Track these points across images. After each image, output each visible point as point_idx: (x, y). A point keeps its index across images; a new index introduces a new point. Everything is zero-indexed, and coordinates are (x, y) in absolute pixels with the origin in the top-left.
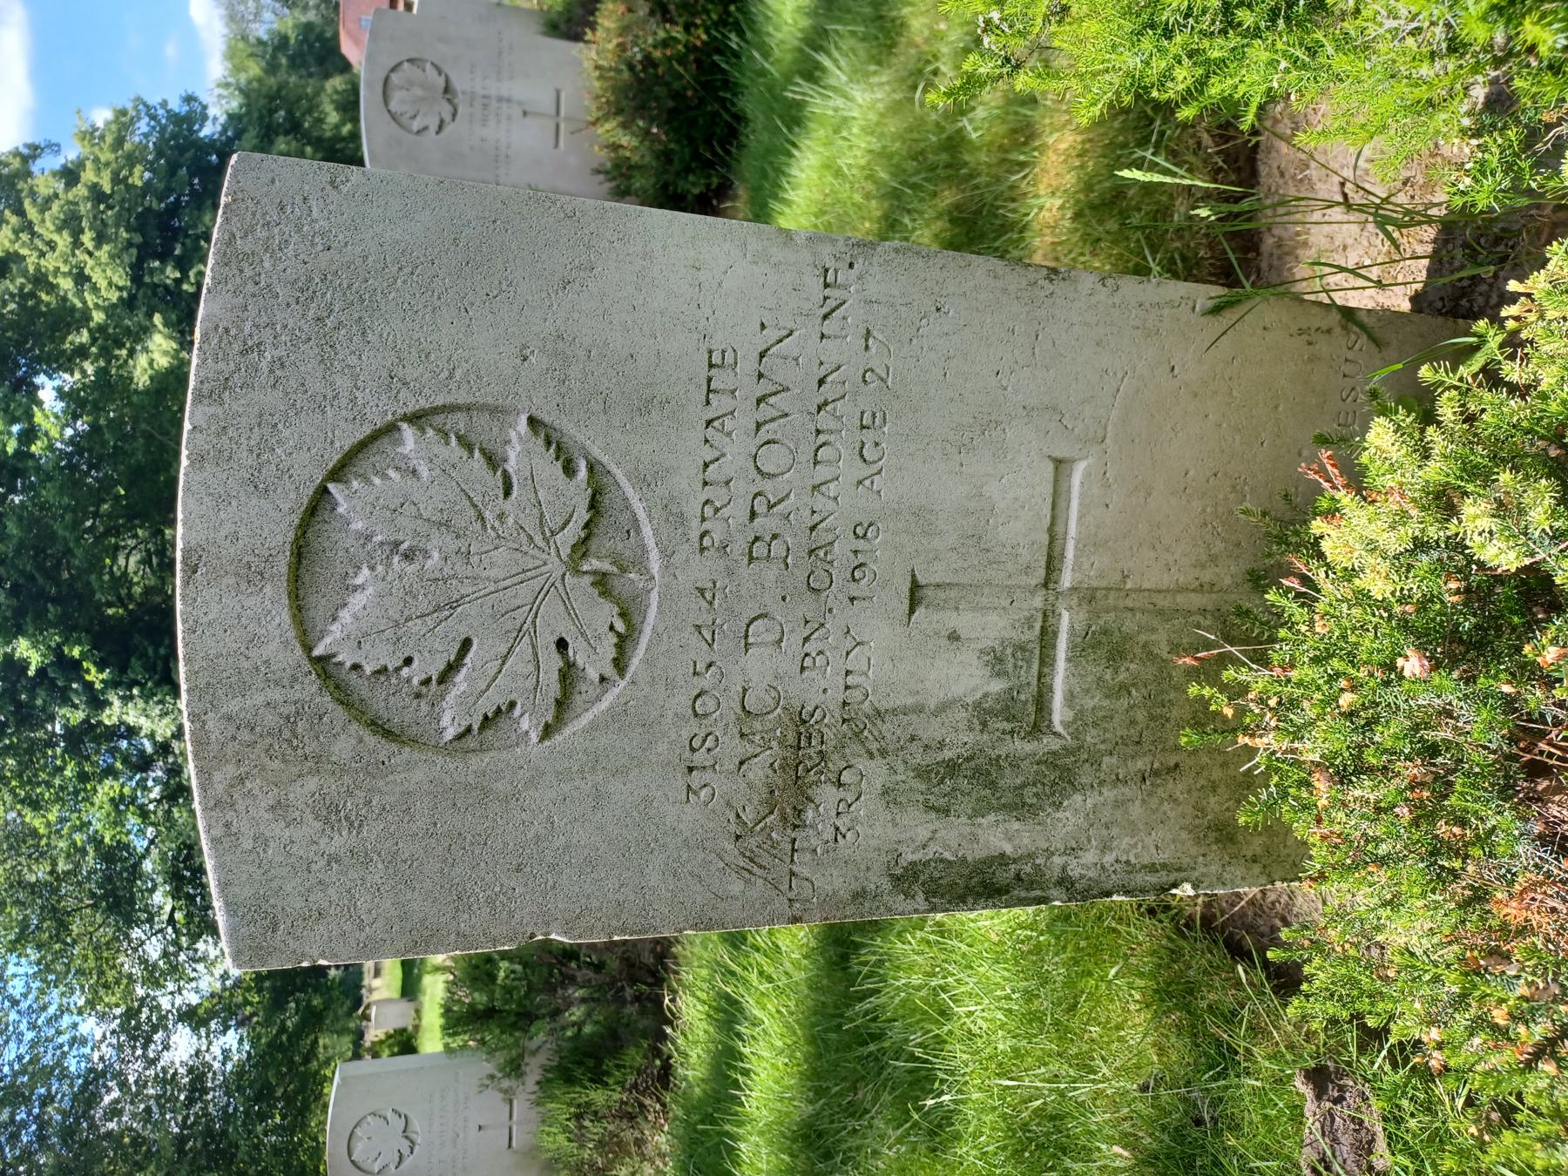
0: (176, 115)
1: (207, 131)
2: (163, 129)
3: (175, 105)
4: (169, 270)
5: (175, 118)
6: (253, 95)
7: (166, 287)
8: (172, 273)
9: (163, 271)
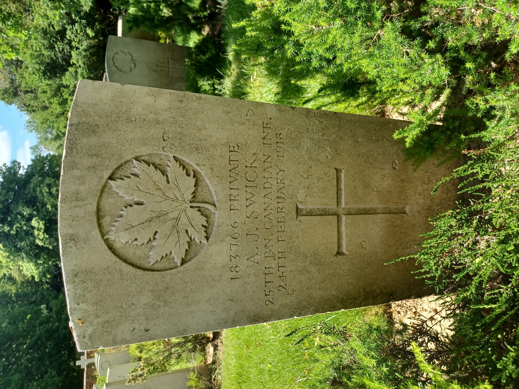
0: (9, 168)
1: (22, 172)
2: (4, 173)
3: (9, 165)
4: (5, 227)
5: (9, 169)
6: (37, 162)
7: (4, 232)
8: (6, 229)
9: (3, 227)
